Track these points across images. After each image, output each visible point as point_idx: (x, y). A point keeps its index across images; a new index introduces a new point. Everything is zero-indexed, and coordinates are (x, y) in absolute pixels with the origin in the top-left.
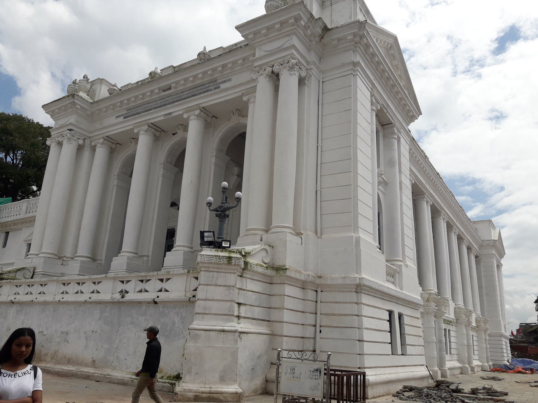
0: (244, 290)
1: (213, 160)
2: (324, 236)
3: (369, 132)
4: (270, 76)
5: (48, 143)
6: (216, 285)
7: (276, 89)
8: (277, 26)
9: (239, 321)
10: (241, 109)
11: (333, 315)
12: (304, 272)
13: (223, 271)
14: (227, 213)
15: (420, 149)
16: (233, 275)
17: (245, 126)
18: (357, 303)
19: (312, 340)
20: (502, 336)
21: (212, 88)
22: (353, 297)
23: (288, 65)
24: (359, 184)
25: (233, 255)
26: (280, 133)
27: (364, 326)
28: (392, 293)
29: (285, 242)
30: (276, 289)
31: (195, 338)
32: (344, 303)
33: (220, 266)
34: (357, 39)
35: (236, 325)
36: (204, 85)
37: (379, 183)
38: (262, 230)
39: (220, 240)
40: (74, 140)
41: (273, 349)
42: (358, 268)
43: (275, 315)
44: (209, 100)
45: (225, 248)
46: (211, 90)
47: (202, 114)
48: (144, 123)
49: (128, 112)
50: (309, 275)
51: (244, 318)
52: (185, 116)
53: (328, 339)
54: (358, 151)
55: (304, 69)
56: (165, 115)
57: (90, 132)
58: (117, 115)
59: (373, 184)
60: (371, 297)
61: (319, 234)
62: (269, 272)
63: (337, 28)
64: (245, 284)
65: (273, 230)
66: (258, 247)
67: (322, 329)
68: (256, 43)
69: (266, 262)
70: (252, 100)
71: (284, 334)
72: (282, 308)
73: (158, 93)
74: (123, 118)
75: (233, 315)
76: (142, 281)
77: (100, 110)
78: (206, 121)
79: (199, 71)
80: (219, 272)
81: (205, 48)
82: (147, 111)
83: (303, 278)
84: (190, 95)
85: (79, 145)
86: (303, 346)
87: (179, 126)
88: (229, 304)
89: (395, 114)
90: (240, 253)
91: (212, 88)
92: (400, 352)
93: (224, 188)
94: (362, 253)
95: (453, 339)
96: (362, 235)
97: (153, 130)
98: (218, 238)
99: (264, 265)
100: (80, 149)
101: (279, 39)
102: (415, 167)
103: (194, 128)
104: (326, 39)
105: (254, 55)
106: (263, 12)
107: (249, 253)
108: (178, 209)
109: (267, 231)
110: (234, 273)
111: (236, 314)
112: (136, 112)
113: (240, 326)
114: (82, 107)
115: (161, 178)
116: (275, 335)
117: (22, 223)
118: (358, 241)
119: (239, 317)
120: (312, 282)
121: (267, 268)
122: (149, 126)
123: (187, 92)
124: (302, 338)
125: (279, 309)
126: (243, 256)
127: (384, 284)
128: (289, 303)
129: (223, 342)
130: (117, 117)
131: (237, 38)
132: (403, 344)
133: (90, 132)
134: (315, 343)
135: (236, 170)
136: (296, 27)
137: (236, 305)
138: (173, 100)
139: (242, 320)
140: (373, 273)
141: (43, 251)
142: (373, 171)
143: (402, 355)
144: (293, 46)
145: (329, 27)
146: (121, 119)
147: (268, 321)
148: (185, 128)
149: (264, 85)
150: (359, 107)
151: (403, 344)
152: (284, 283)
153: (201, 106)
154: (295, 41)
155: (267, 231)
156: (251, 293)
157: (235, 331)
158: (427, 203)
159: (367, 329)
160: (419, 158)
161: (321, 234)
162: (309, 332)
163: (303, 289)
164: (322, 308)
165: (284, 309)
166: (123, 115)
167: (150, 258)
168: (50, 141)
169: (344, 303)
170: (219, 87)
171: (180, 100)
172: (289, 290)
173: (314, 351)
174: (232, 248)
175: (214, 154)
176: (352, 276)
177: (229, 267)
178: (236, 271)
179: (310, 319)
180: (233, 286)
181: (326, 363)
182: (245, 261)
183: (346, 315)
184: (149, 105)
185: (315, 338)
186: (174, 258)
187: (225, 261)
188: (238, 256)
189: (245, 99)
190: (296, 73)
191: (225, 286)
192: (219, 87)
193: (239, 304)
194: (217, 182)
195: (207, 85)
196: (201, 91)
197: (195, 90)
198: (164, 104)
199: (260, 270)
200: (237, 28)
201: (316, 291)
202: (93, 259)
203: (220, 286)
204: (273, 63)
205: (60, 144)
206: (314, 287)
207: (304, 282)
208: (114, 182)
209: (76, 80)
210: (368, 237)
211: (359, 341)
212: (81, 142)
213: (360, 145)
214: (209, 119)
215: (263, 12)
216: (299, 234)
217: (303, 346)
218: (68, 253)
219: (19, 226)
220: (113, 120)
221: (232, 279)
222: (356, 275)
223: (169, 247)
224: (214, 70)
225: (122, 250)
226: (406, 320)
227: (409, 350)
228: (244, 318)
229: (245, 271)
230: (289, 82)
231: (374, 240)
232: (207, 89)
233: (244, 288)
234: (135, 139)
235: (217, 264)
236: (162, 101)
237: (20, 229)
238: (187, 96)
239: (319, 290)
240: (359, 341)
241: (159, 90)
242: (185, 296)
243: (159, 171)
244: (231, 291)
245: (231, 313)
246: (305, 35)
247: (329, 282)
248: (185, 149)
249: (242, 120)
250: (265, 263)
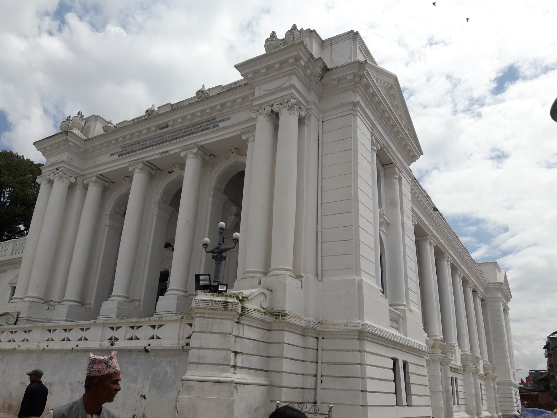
0: (241, 337)
1: (211, 199)
2: (324, 279)
3: (370, 172)
4: (269, 116)
5: (38, 181)
6: (211, 333)
7: (276, 128)
8: (277, 66)
9: (236, 372)
10: (240, 147)
11: (335, 363)
12: (304, 318)
13: (219, 317)
14: (224, 254)
15: (422, 189)
16: (229, 321)
17: (244, 165)
18: (359, 351)
19: (312, 392)
20: (511, 384)
22: (356, 344)
23: (287, 104)
24: (361, 225)
25: (229, 300)
26: (279, 173)
27: (368, 376)
28: (396, 340)
29: (284, 286)
30: (275, 337)
31: (189, 389)
32: (346, 351)
33: (216, 312)
34: (357, 79)
35: (233, 375)
36: (202, 123)
37: (381, 224)
38: (260, 273)
39: (216, 284)
40: (65, 178)
41: (271, 401)
42: (361, 314)
43: (273, 365)
45: (221, 292)
46: (209, 128)
47: (200, 152)
48: (139, 161)
49: (123, 149)
50: (309, 321)
51: (241, 367)
52: (182, 154)
53: (329, 389)
54: (359, 190)
55: (303, 108)
56: (161, 153)
57: (83, 170)
58: (112, 152)
59: (374, 225)
60: (374, 344)
61: (320, 277)
62: (268, 318)
63: (336, 68)
64: (241, 331)
65: (271, 273)
66: (256, 291)
67: (323, 379)
68: (256, 82)
69: (264, 307)
70: (251, 139)
71: (283, 385)
72: (281, 357)
73: (155, 131)
75: (229, 365)
76: (133, 328)
78: (204, 159)
79: (197, 109)
80: (215, 318)
81: (203, 86)
82: (143, 148)
83: (303, 324)
84: (188, 133)
85: (71, 183)
86: (303, 398)
88: (224, 352)
89: (396, 154)
90: (237, 297)
91: (211, 126)
92: (405, 403)
93: (222, 229)
94: (365, 298)
95: (460, 389)
96: (365, 278)
97: (149, 168)
98: (214, 281)
99: (262, 310)
100: (71, 187)
101: (279, 78)
102: (417, 207)
103: (191, 167)
104: (326, 80)
105: (253, 94)
106: (263, 52)
107: (246, 298)
108: (173, 250)
109: (265, 274)
110: (230, 319)
111: (232, 363)
112: (131, 150)
113: (237, 376)
114: (75, 144)
115: (155, 218)
116: (273, 386)
117: (7, 265)
118: (360, 283)
119: (235, 367)
120: (313, 329)
121: (265, 313)
122: (144, 165)
123: (185, 130)
124: (302, 388)
125: (278, 357)
126: (240, 300)
127: (388, 330)
128: (288, 352)
129: (218, 394)
130: (111, 155)
131: (237, 76)
132: (408, 394)
133: (83, 170)
134: (316, 395)
135: (234, 209)
136: (295, 66)
137: (233, 354)
138: (169, 139)
139: (238, 370)
140: (376, 318)
141: (29, 294)
142: (374, 212)
143: (407, 405)
144: (293, 86)
145: (329, 67)
147: (267, 371)
148: (182, 166)
149: (263, 125)
150: (360, 147)
151: (408, 394)
152: (284, 330)
153: (199, 144)
154: (295, 81)
155: (265, 274)
156: (248, 340)
157: (231, 382)
158: (430, 244)
159: (371, 378)
160: (421, 198)
161: (322, 278)
162: (310, 382)
163: (304, 336)
164: (324, 357)
165: (283, 358)
166: (117, 153)
167: (142, 303)
168: (41, 179)
169: (346, 351)
170: (218, 126)
171: (177, 138)
172: (289, 337)
173: (315, 403)
174: (229, 292)
175: (212, 193)
176: (355, 322)
177: (225, 312)
178: (232, 318)
179: (311, 368)
180: (230, 334)
181: (327, 416)
182: (242, 307)
183: (348, 364)
184: (145, 142)
185: (315, 389)
186: (167, 303)
187: (222, 306)
188: (235, 300)
189: (244, 137)
190: (296, 112)
191: (221, 333)
192: (218, 126)
193: (236, 353)
194: (214, 223)
195: (206, 124)
196: (199, 129)
199: (258, 315)
200: (237, 67)
201: (317, 338)
202: (82, 303)
203: (216, 333)
204: (272, 103)
205: (51, 182)
206: (315, 334)
207: (305, 329)
208: (106, 221)
209: (70, 117)
210: (370, 280)
211: (362, 391)
212: (73, 180)
213: (361, 184)
214: (207, 158)
215: (263, 52)
216: (299, 277)
217: (303, 398)
218: (55, 297)
220: (107, 158)
221: (228, 325)
222: (359, 321)
223: (162, 291)
224: (213, 108)
226: (411, 368)
227: (415, 400)
228: (241, 367)
229: (242, 317)
230: (289, 121)
231: (377, 283)
232: (205, 127)
233: (241, 336)
234: (130, 177)
235: (213, 309)
236: (159, 139)
237: (5, 271)
238: (184, 134)
239: (320, 337)
240: (362, 391)
241: (156, 128)
242: (178, 344)
243: (154, 211)
244: (227, 339)
245: (227, 363)
246: (305, 75)
247: (331, 328)
248: (181, 188)
249: (241, 159)
250: (264, 308)
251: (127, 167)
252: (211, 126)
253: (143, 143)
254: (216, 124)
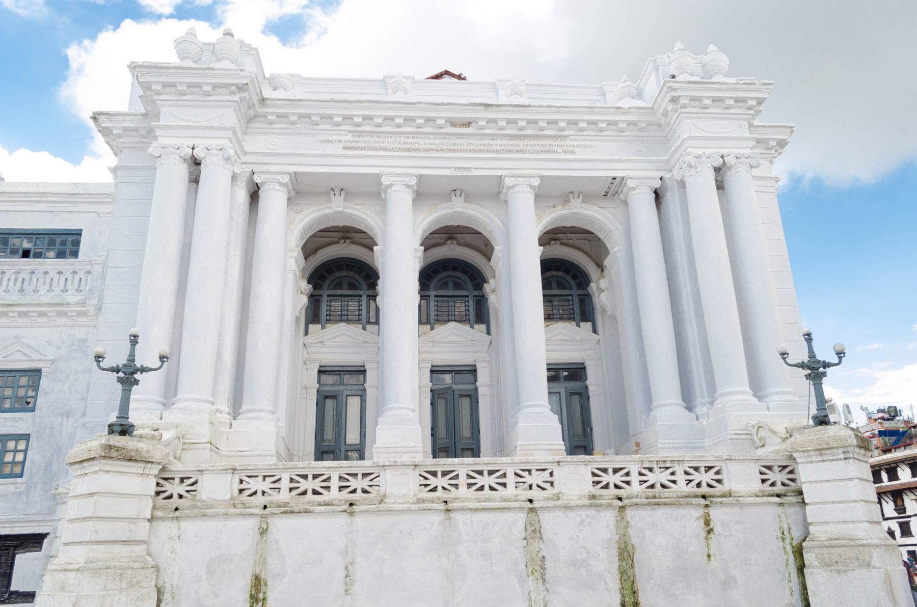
21: (560, 149)
23: (748, 160)
49: (354, 139)
74: (341, 145)
87: (458, 192)
112: (377, 145)
123: (505, 142)
138: (472, 148)
146: (337, 149)
166: (341, 142)
192: (573, 152)
196: (536, 148)
197: (522, 143)
198: (447, 147)
232: (547, 148)
238: (503, 148)
251: (378, 177)
252: (560, 149)
253: (407, 140)
254: (570, 149)
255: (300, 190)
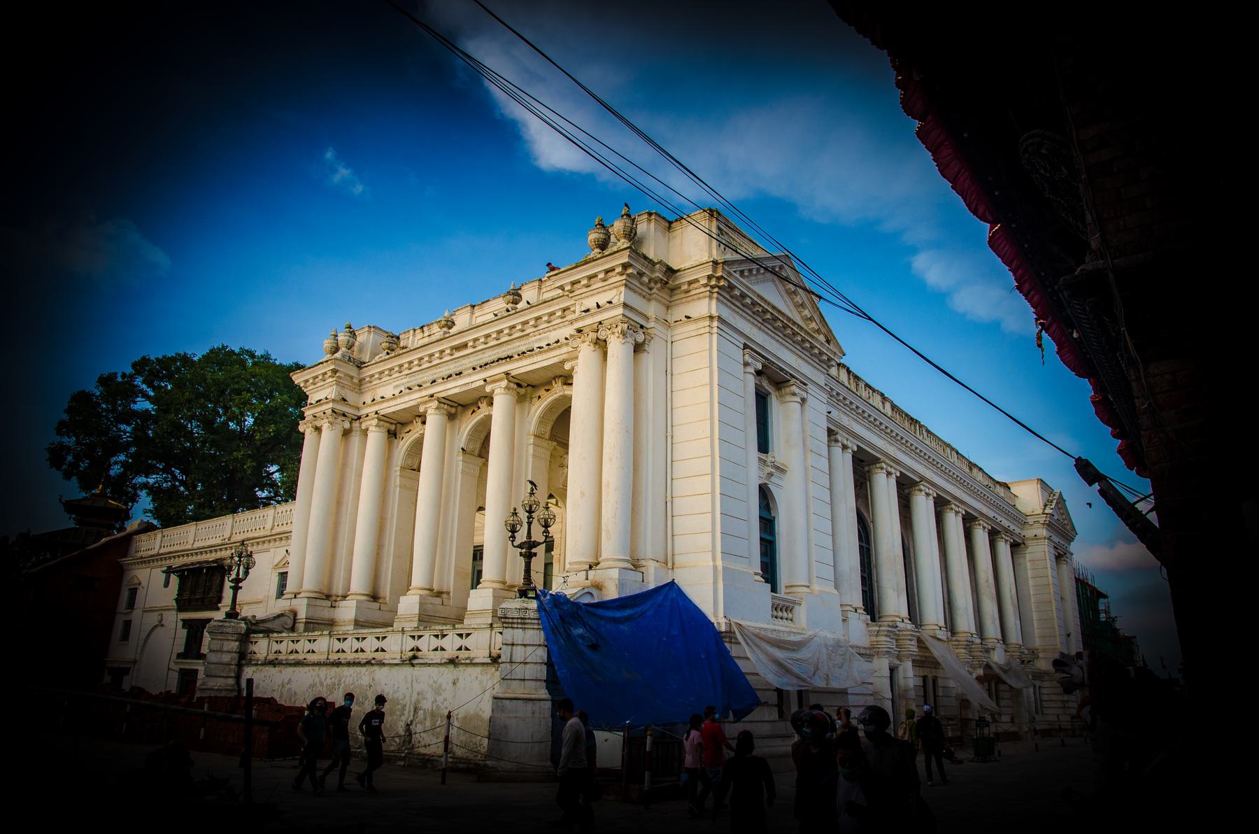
5: (301, 429)
14: (533, 550)
44: (520, 367)
52: (488, 389)
77: (372, 376)
100: (346, 433)
114: (346, 375)
149: (586, 357)
189: (567, 366)
205: (318, 429)
212: (347, 425)
219: (266, 545)
225: (413, 584)
246: (641, 284)
255: (395, 427)
